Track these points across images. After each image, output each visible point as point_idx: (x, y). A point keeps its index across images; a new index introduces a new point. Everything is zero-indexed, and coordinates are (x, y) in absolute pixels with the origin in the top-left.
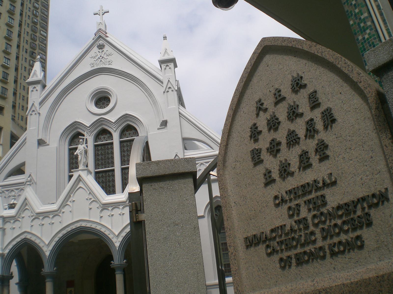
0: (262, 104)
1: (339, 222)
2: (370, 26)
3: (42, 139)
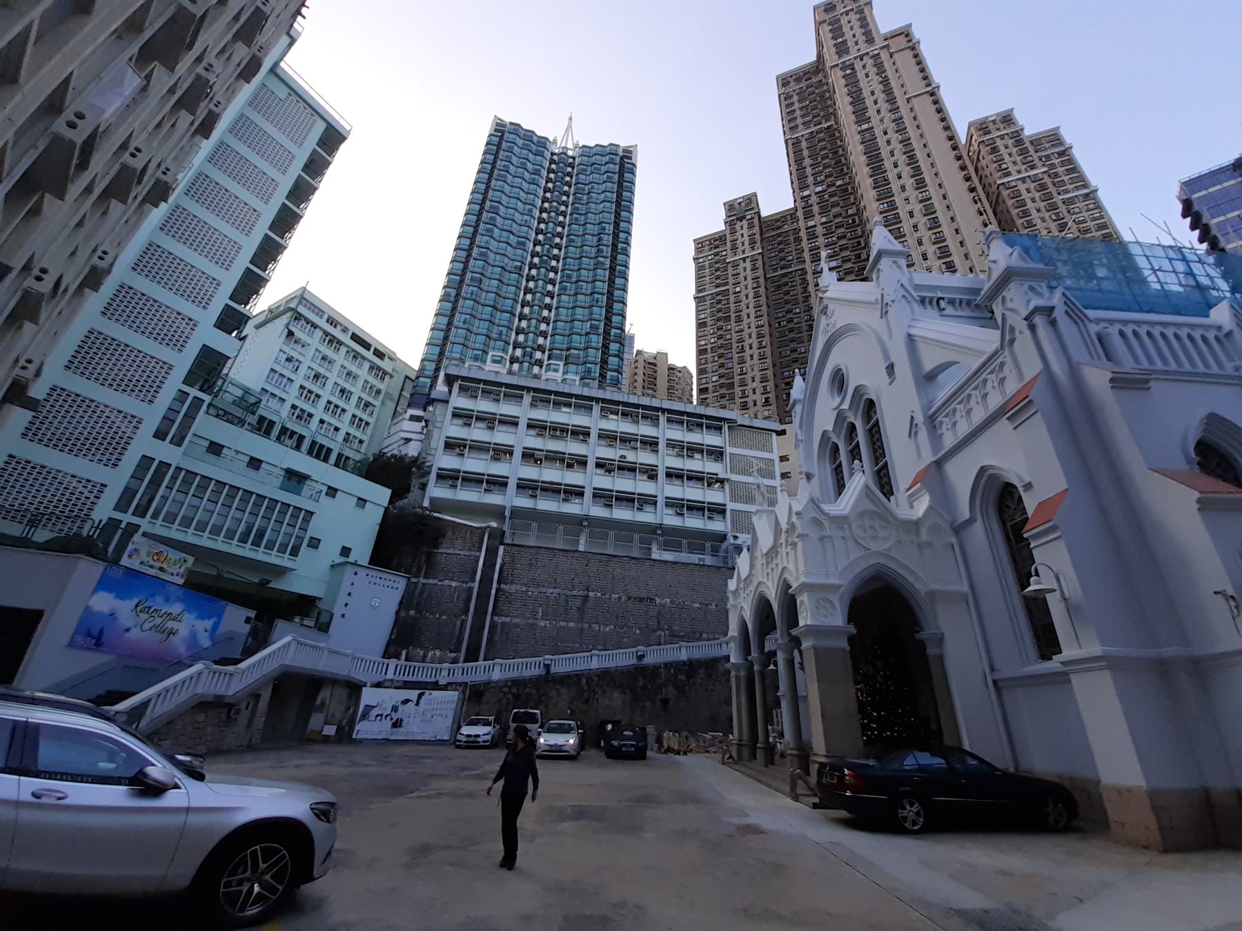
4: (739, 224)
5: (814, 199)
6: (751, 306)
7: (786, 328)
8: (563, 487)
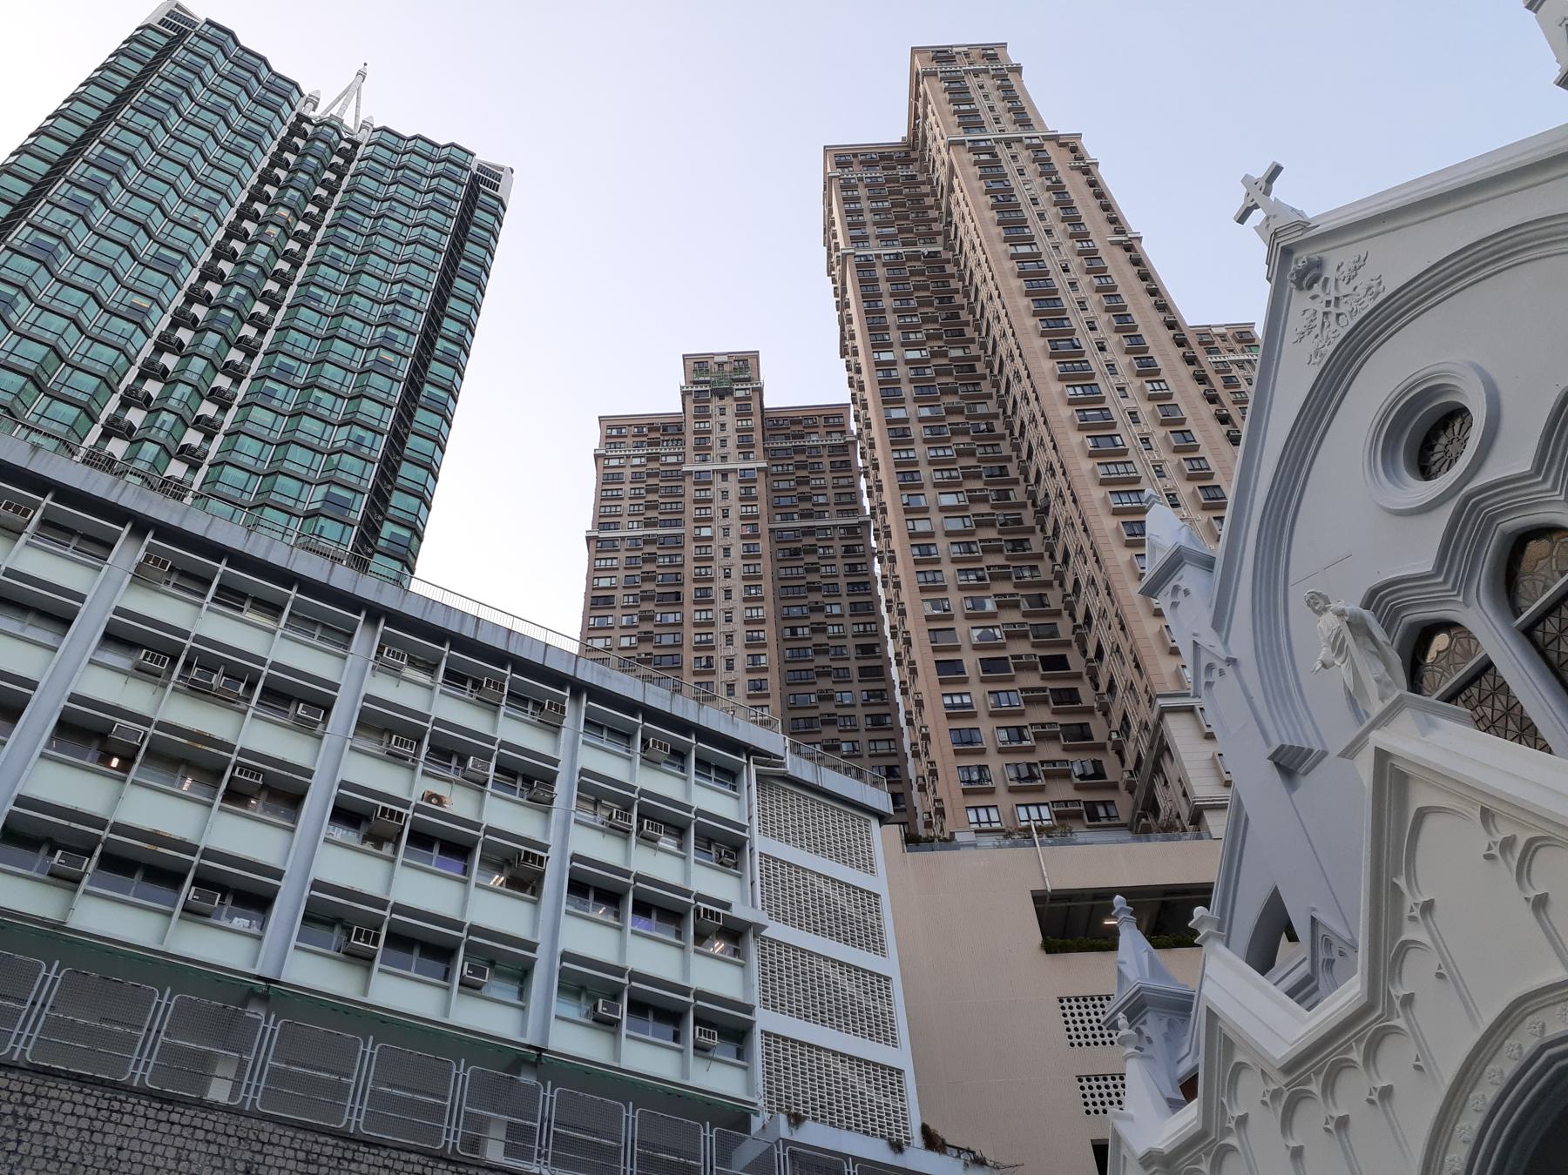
3: (1282, 747)
4: (715, 404)
5: (902, 371)
6: (736, 573)
7: (809, 644)
8: (196, 860)
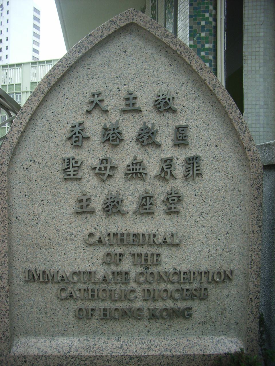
0: (101, 101)
1: (170, 287)
2: (211, 61)
